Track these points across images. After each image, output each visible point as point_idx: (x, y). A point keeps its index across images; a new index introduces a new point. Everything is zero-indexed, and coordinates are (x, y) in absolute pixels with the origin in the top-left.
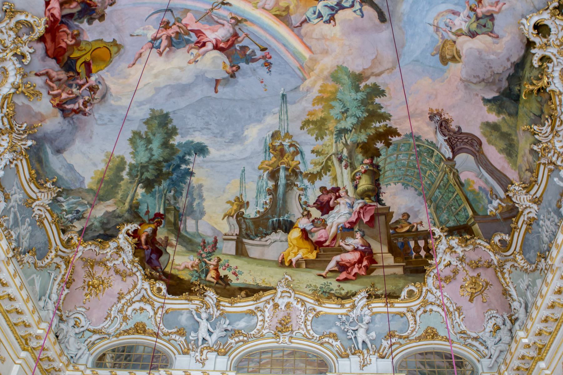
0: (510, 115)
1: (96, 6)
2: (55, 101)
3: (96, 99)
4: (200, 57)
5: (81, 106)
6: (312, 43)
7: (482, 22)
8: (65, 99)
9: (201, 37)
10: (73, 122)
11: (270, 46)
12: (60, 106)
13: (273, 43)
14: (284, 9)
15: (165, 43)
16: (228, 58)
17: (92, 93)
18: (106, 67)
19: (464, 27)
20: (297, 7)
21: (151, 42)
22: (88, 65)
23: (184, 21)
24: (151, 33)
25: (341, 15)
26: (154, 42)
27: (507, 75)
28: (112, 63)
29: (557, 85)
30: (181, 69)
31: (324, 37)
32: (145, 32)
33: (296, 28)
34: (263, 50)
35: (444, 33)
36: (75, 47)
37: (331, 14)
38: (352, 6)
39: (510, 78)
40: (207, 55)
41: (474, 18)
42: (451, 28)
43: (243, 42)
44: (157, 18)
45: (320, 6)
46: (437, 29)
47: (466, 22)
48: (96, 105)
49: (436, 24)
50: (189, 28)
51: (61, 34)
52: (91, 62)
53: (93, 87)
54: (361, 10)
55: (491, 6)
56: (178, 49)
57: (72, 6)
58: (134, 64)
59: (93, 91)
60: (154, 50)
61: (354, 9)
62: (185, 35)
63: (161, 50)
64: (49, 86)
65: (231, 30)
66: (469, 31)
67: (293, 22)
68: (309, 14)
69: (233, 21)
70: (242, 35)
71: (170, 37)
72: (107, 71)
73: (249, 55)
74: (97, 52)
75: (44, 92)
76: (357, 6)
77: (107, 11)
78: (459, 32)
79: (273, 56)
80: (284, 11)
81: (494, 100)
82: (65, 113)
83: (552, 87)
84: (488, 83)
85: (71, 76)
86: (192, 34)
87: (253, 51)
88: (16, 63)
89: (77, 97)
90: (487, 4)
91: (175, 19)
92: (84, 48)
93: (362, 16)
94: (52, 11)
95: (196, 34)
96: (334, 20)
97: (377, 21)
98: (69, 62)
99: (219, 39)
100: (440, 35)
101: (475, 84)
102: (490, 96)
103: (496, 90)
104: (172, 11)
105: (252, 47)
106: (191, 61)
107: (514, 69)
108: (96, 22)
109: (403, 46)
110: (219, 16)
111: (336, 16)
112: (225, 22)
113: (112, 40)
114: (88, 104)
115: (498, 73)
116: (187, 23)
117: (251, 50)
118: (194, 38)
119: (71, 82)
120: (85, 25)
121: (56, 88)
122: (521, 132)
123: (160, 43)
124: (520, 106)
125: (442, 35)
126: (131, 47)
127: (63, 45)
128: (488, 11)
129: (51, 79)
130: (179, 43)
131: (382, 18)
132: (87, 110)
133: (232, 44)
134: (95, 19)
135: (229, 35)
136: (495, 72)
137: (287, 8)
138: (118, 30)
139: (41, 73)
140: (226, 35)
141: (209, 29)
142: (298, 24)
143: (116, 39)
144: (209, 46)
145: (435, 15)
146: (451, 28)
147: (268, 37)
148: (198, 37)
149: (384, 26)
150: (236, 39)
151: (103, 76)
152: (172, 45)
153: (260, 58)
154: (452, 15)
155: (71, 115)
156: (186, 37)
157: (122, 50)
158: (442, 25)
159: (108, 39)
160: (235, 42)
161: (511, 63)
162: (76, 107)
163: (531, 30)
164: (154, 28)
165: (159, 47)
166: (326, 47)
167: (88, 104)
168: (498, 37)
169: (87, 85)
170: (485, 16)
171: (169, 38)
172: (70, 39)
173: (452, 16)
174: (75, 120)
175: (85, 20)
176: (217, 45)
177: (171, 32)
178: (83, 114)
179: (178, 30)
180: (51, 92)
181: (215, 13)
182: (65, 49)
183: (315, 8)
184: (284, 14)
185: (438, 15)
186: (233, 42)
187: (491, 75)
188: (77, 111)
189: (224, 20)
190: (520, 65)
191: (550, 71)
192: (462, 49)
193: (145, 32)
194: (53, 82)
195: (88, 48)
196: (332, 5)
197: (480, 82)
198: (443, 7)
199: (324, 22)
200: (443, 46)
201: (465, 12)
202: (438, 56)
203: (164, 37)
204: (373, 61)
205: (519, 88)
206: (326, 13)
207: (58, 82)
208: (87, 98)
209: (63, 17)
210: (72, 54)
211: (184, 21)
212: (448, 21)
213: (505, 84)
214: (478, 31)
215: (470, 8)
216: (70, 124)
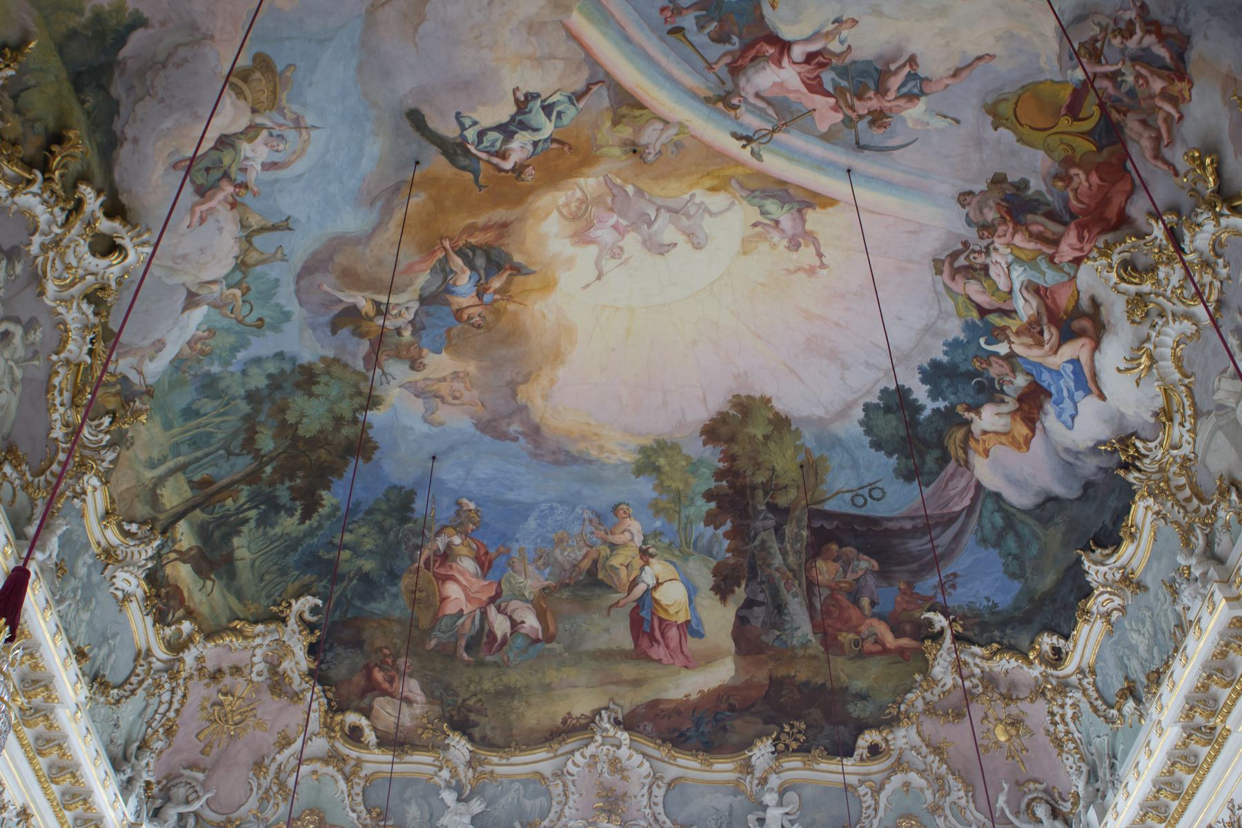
0: (73, 34)
1: (998, 204)
2: (1181, 91)
3: (1099, 24)
4: (825, 30)
5: (1138, 30)
6: (564, 48)
7: (216, 174)
8: (1160, 77)
9: (811, 76)
10: (1178, 11)
11: (662, 39)
12: (1178, 70)
13: (653, 46)
14: (624, 120)
15: (894, 83)
16: (762, 17)
17: (1098, 45)
18: (1041, 83)
19: (245, 148)
20: (596, 126)
21: (923, 93)
22: (1074, 110)
23: (839, 117)
24: (915, 112)
25: (505, 112)
26: (917, 88)
27: (122, 110)
28: (1025, 83)
29: (29, 200)
30: (877, 11)
31: (539, 61)
32: (926, 118)
33: (600, 78)
34: (677, 31)
35: (282, 121)
36: (1077, 159)
37: (525, 113)
38: (481, 134)
39: (113, 108)
40: (810, 32)
41: (234, 171)
42: (271, 135)
43: (722, 51)
44: (891, 138)
45: (548, 129)
46: (298, 124)
47: (246, 158)
48: (1108, 12)
49: (303, 131)
50: (832, 101)
51: (1086, 201)
52: (1063, 111)
53: (1091, 55)
54: (463, 128)
55: (210, 209)
56: (870, 62)
57: (1041, 228)
58: (979, 58)
59: (1095, 48)
60: (922, 72)
61: (477, 128)
62: (844, 88)
63: (907, 69)
64: (1169, 130)
65: (742, 82)
66: (233, 146)
67: (605, 92)
68: (570, 113)
69: (735, 101)
70: (721, 69)
71: (877, 92)
72: (1041, 71)
73: (712, 20)
74: (1041, 125)
75: (1191, 130)
76: (471, 134)
77: (984, 187)
78: (251, 134)
79: (656, 13)
80: (624, 116)
81: (121, 40)
82: (1180, 45)
83: (35, 188)
84: (155, 65)
85: (1118, 111)
86: (829, 87)
87: (701, 27)
88: (1187, 239)
89: (1135, 59)
90: (219, 207)
91: (855, 127)
92: (1062, 147)
93: (458, 116)
94: (1079, 246)
95: (821, 84)
96: (517, 101)
97: (426, 111)
98: (1104, 142)
99: (773, 66)
100: (289, 115)
101: (178, 45)
102: (137, 39)
103: (129, 63)
104: (857, 143)
105: (701, 39)
106: (849, 24)
107: (114, 133)
108: (1013, 177)
109: (360, 68)
110: (762, 114)
111: (513, 109)
112: (752, 100)
113: (1002, 130)
114: (1122, 25)
115: (142, 99)
116: (833, 113)
117: (706, 31)
118: (828, 77)
119: (1126, 99)
120: (1036, 185)
121: (1161, 116)
122: (34, 28)
123: (903, 85)
124: (63, 75)
125: (284, 116)
126: (968, 100)
127: (1094, 179)
128: (212, 198)
129: (1158, 139)
130: (863, 73)
131: (416, 119)
132: (1131, 14)
133: (746, 48)
134: (1012, 184)
135: (750, 72)
136: (148, 98)
137: (615, 123)
138: (979, 142)
139: (1165, 167)
140: (757, 72)
141: (789, 91)
142: (595, 88)
143: (990, 129)
144: (798, 52)
145: (310, 149)
146: (271, 135)
147: (662, 60)
148: (818, 76)
149: (411, 103)
150: (734, 61)
151: (1056, 63)
152: (880, 72)
153: (687, 9)
154: (276, 160)
155: (1173, 31)
156: (844, 83)
157: (990, 100)
158: (291, 134)
159: (1006, 135)
160: (738, 54)
161: (126, 139)
162: (1150, 40)
163: (126, 242)
164: (904, 120)
165: (912, 76)
166: (533, 39)
167: (1122, 25)
168: (175, 166)
169: (1099, 69)
170: (216, 186)
171: (881, 91)
172: (1076, 180)
173: (276, 158)
174: (1173, 12)
175: (1030, 192)
176: (781, 54)
177: (874, 104)
178: (1148, 12)
179: (857, 103)
180: (1177, 116)
181: (769, 121)
182: (1097, 170)
183: (559, 124)
184: (624, 110)
185: (303, 150)
186: (742, 56)
187: (153, 86)
188: (1153, 26)
189: (753, 105)
190: (109, 146)
191: (57, 210)
192: (233, 104)
193: (926, 118)
194: (1159, 130)
195: (1053, 141)
196: (524, 133)
197: (170, 55)
198: (299, 167)
199: (538, 96)
200: (274, 92)
201: (255, 174)
202: (279, 69)
203: (891, 95)
204: (421, 17)
205: (87, 106)
206: (537, 116)
207: (1150, 121)
208: (1116, 42)
209: (1066, 224)
210: (1091, 152)
211: (839, 117)
212: (281, 147)
213: (117, 89)
214: (215, 154)
215: (246, 187)
216: (1187, 14)
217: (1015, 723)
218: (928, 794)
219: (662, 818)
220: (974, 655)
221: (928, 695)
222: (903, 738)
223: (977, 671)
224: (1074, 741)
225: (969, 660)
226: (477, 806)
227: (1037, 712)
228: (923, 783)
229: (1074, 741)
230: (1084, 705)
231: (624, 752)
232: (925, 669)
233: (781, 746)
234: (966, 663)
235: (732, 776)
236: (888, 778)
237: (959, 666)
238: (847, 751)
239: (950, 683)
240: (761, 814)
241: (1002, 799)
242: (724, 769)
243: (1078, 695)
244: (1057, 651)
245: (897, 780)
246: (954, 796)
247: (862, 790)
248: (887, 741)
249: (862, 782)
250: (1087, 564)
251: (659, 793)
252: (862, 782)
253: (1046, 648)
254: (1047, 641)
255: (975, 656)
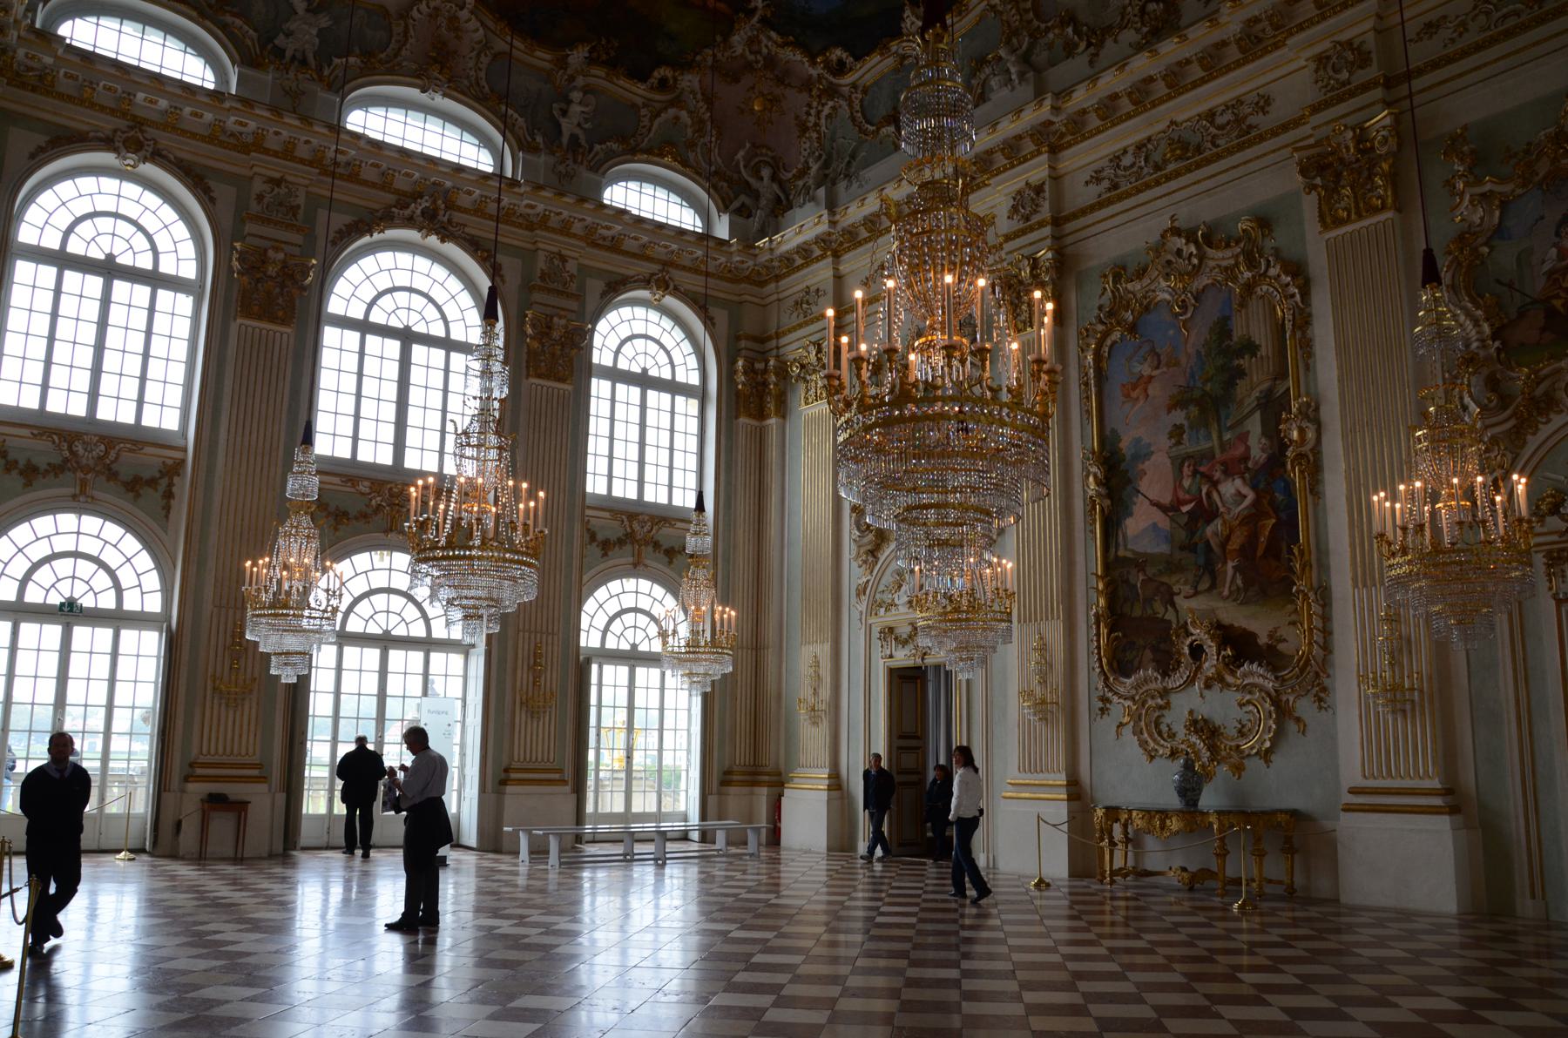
217: (773, 101)
218: (689, 131)
219: (483, 83)
220: (770, 38)
221: (719, 55)
222: (689, 81)
223: (765, 51)
224: (818, 132)
225: (765, 41)
226: (324, 21)
227: (796, 100)
228: (689, 122)
229: (818, 132)
230: (845, 111)
231: (464, 14)
232: (726, 36)
233: (595, 55)
234: (760, 42)
235: (547, 65)
236: (666, 109)
237: (752, 42)
238: (640, 75)
239: (739, 51)
240: (563, 105)
241: (741, 153)
242: (543, 58)
243: (844, 103)
244: (841, 63)
245: (672, 112)
246: (707, 139)
247: (644, 112)
248: (675, 80)
249: (645, 105)
250: (908, 13)
251: (485, 60)
252: (645, 105)
253: (834, 57)
254: (838, 53)
255: (770, 41)
